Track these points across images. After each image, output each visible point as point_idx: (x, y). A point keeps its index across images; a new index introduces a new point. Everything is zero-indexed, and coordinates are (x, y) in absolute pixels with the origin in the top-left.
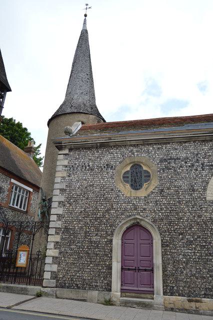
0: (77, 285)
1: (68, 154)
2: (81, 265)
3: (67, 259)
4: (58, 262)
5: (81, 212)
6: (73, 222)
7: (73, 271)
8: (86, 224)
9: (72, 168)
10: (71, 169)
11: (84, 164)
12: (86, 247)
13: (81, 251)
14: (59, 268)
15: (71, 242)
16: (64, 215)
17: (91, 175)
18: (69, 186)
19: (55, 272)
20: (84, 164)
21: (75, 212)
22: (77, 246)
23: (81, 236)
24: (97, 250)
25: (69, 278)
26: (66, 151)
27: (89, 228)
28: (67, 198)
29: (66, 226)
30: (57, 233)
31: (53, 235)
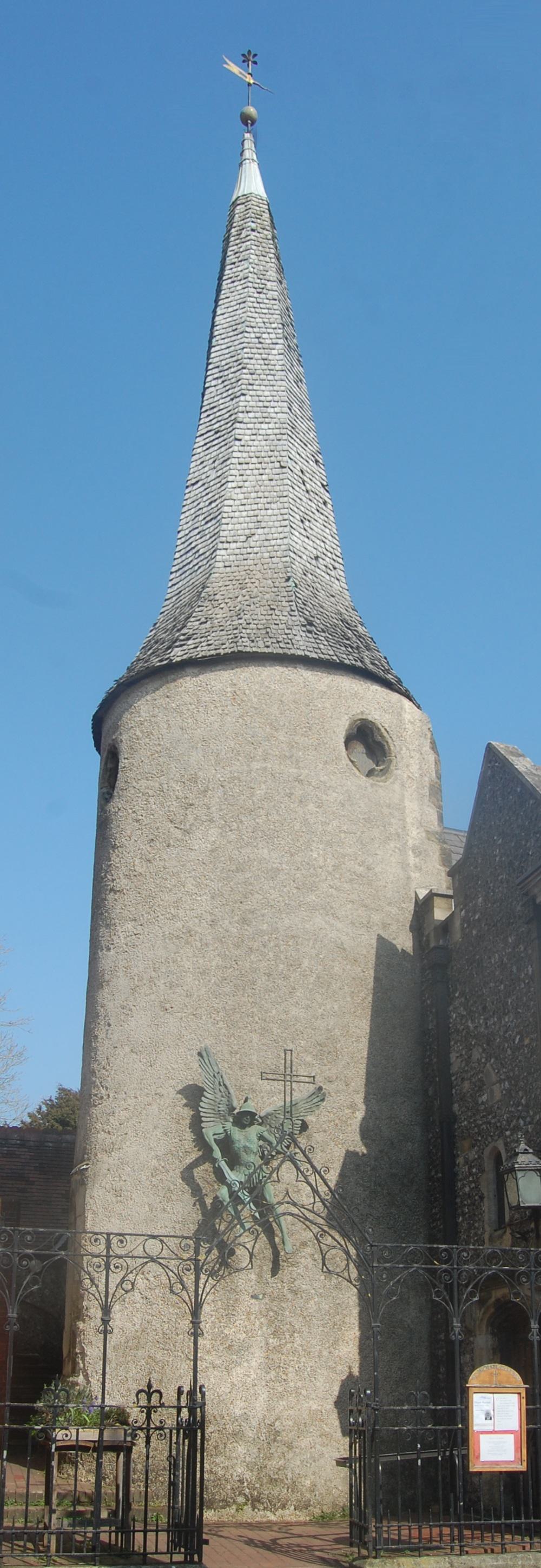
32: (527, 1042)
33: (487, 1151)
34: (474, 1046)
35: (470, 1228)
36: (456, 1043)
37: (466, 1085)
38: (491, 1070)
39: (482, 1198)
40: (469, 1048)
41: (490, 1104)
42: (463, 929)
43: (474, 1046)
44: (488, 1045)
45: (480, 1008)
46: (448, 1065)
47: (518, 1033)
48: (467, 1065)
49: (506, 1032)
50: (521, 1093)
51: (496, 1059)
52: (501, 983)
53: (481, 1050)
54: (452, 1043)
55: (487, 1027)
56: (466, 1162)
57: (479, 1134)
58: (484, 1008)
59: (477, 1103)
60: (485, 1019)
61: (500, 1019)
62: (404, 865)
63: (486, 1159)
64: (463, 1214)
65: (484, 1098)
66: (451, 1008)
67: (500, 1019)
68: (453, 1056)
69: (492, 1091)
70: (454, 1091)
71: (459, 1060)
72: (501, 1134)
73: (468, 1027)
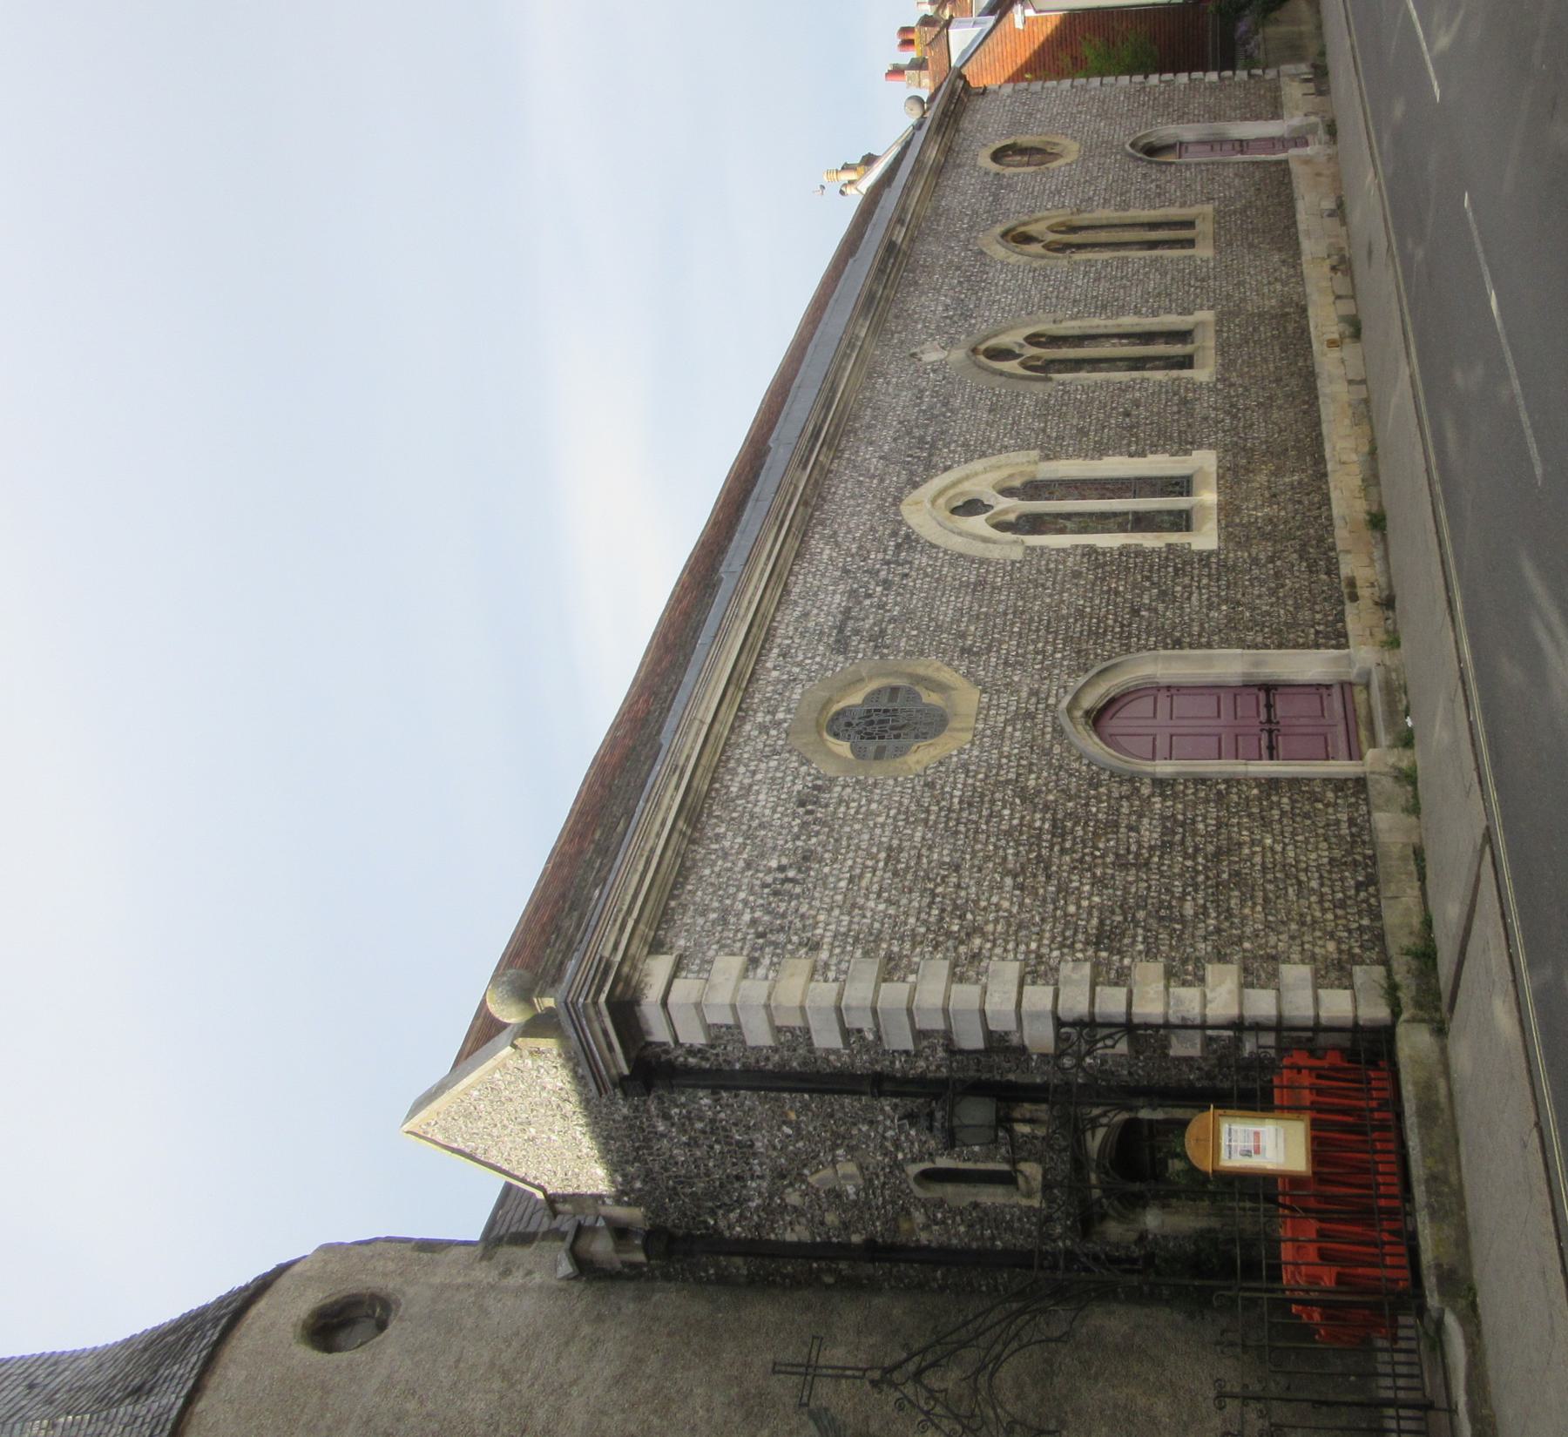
0: (1359, 886)
1: (680, 958)
2: (1270, 876)
3: (1248, 930)
4: (1269, 967)
5: (1022, 887)
6: (1066, 915)
7: (1303, 902)
8: (1079, 866)
9: (772, 937)
10: (766, 944)
11: (765, 885)
12: (1189, 863)
13: (1207, 878)
14: (1296, 957)
15: (1166, 916)
16: (1028, 952)
17: (834, 861)
18: (869, 942)
19: (1316, 973)
20: (768, 886)
21: (1015, 910)
22: (1185, 894)
23: (1138, 880)
24: (1201, 826)
25: (1336, 917)
26: (658, 968)
27: (1103, 857)
28: (936, 948)
29: (1087, 943)
30: (1121, 977)
31: (1130, 993)
32: (793, 1116)
33: (919, 1192)
34: (782, 1199)
35: (1010, 1228)
36: (773, 1230)
37: (830, 1218)
38: (817, 1176)
39: (976, 1205)
40: (784, 1207)
41: (860, 1181)
42: (629, 1204)
43: (782, 1199)
44: (784, 1177)
45: (737, 1185)
46: (799, 1245)
47: (779, 1129)
48: (804, 1215)
49: (774, 1148)
50: (854, 1132)
51: (805, 1166)
52: (711, 1147)
53: (790, 1190)
54: (772, 1236)
55: (761, 1177)
56: (926, 1227)
57: (894, 1203)
58: (738, 1178)
59: (855, 1203)
60: (752, 1179)
61: (755, 1155)
62: (521, 1291)
63: (929, 1195)
64: (993, 1238)
65: (851, 1189)
66: (727, 1234)
67: (755, 1155)
68: (790, 1237)
69: (845, 1177)
70: (834, 1240)
71: (797, 1228)
72: (898, 1166)
73: (758, 1207)
